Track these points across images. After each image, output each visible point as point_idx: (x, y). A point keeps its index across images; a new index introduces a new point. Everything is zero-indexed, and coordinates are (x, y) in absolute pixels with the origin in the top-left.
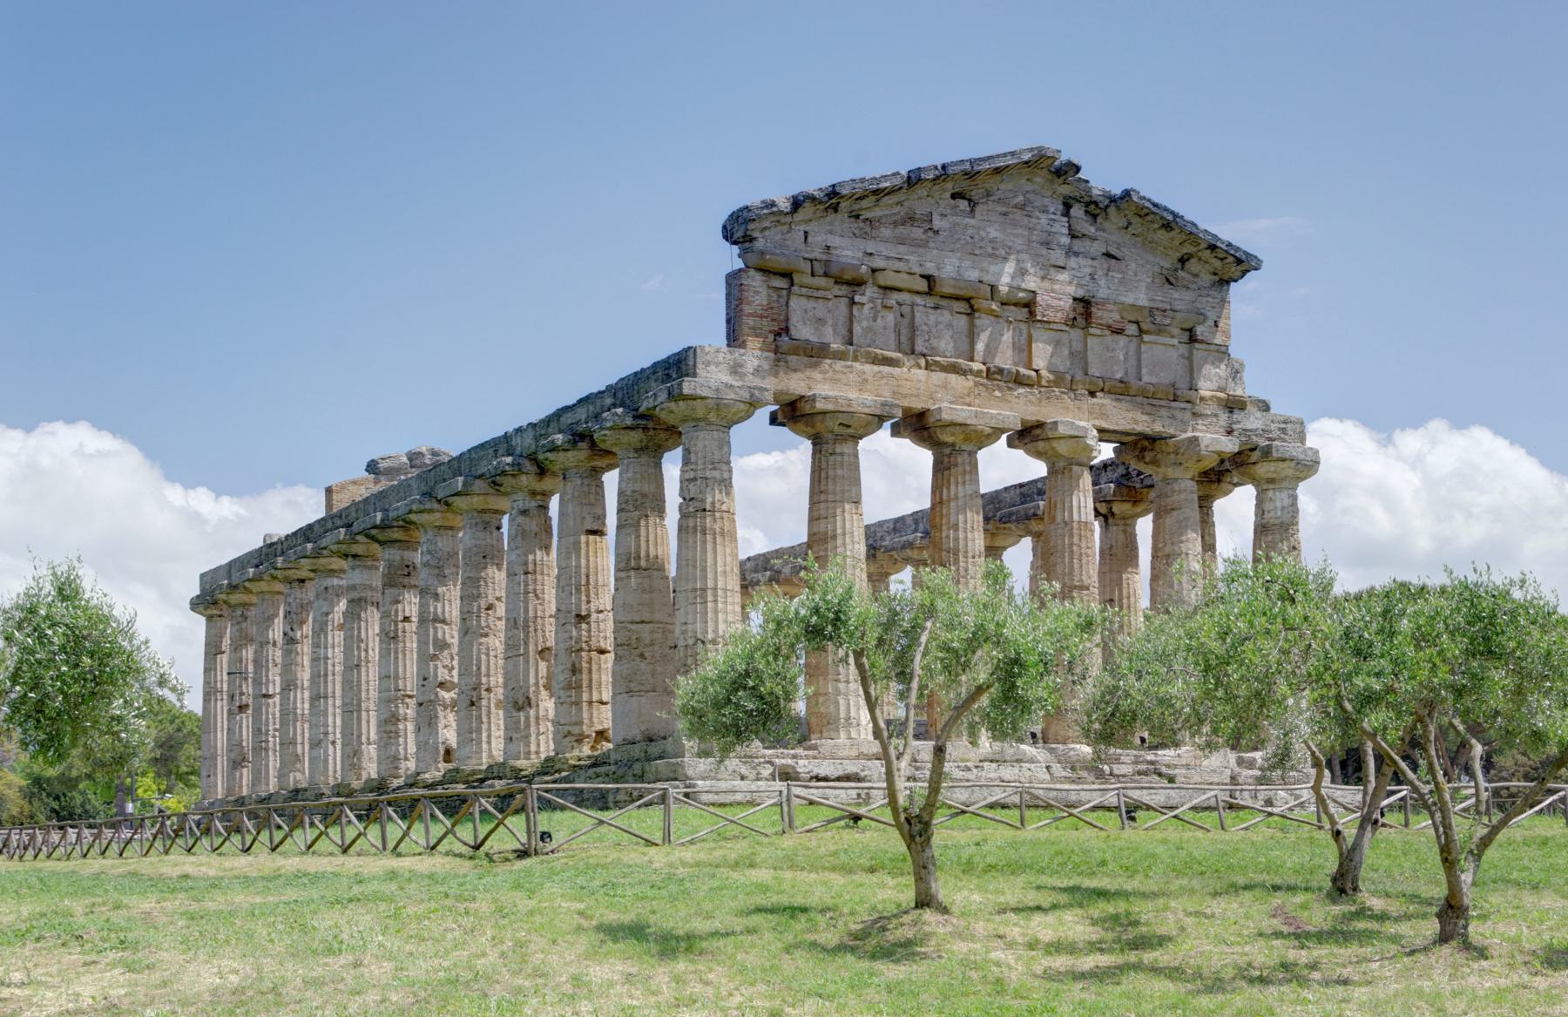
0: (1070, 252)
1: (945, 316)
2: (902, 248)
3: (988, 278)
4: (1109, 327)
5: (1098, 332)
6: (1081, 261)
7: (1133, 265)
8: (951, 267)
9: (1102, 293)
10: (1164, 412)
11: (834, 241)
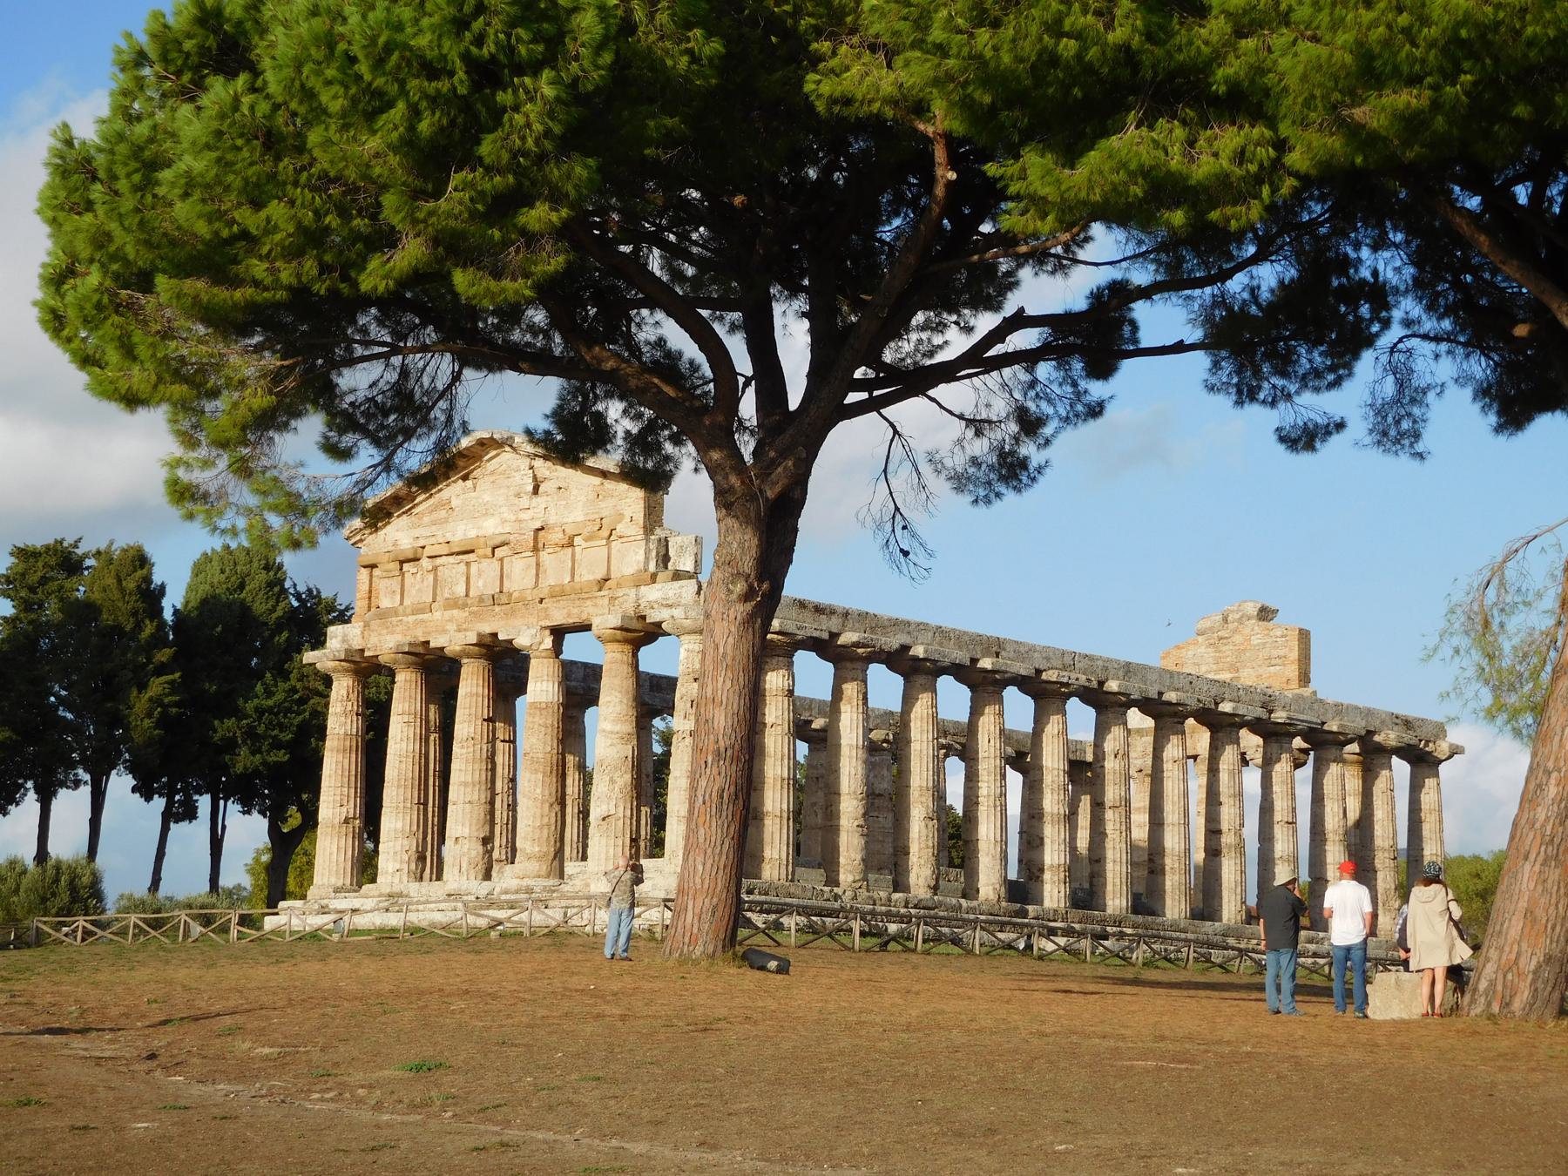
7: (575, 492)
8: (461, 532)
10: (589, 603)
11: (399, 535)
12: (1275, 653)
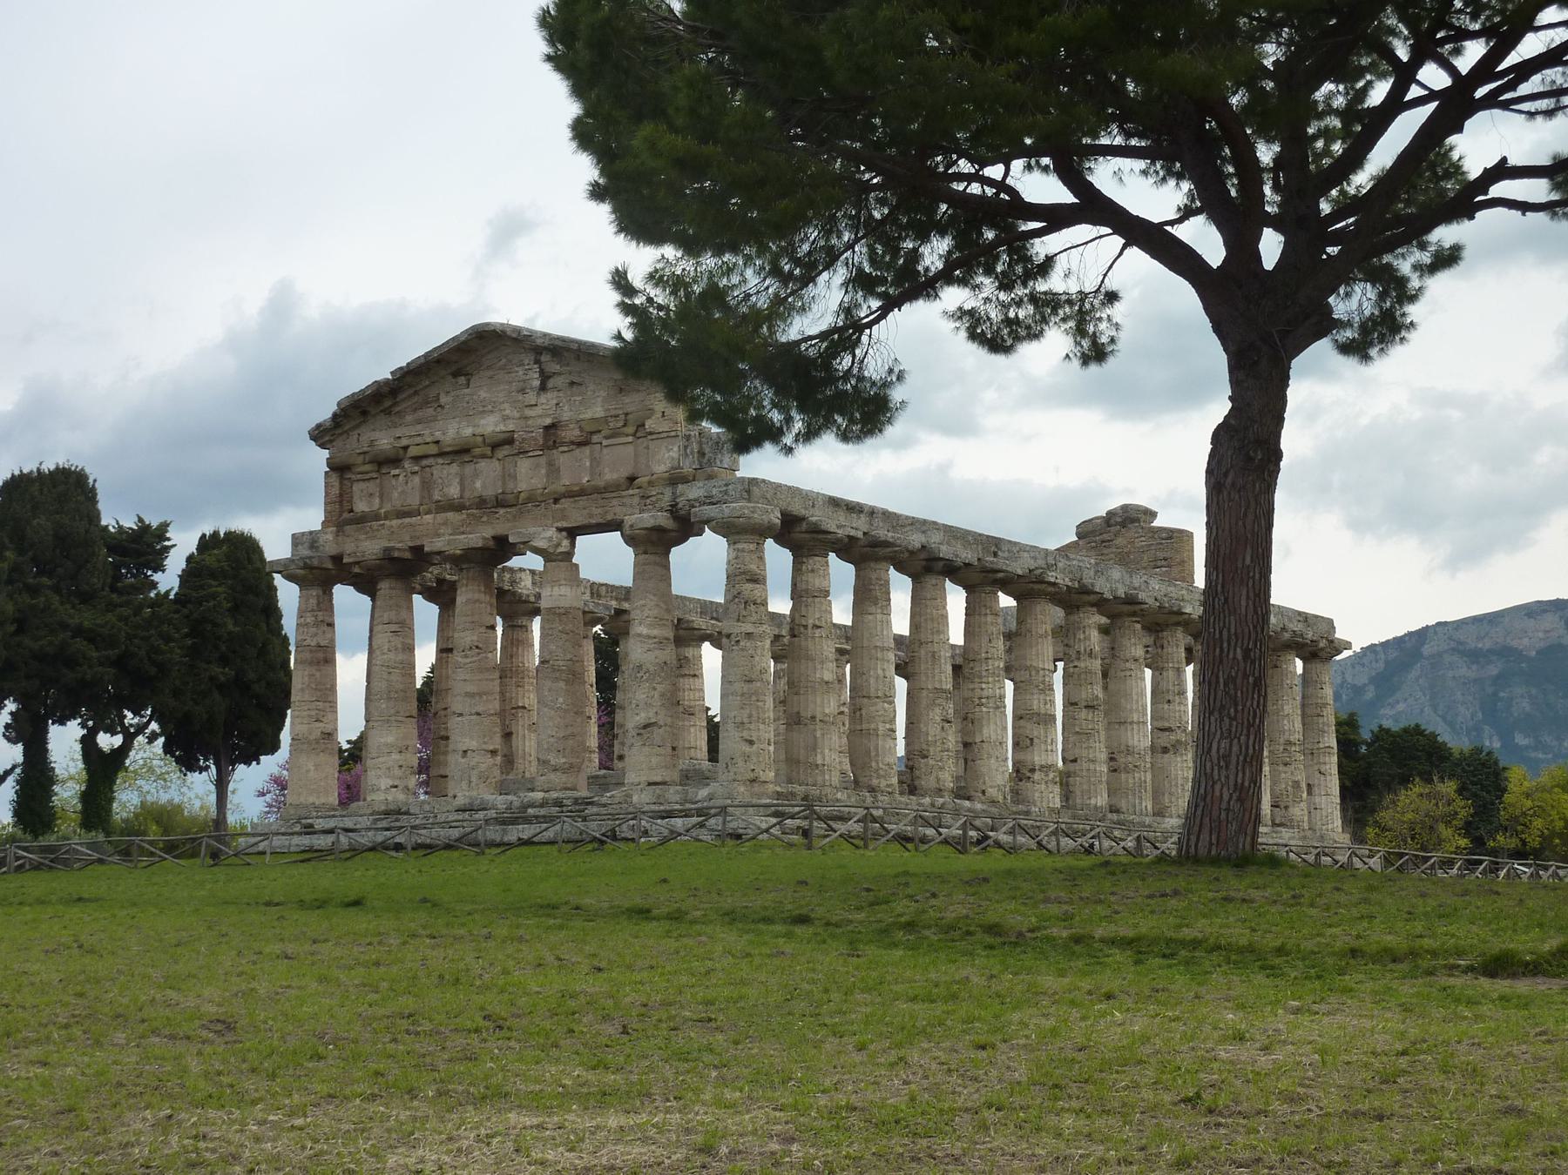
0: (543, 388)
1: (454, 468)
2: (419, 427)
3: (479, 431)
4: (572, 443)
6: (549, 395)
7: (592, 387)
8: (453, 430)
9: (566, 415)
10: (615, 502)
12: (1160, 555)
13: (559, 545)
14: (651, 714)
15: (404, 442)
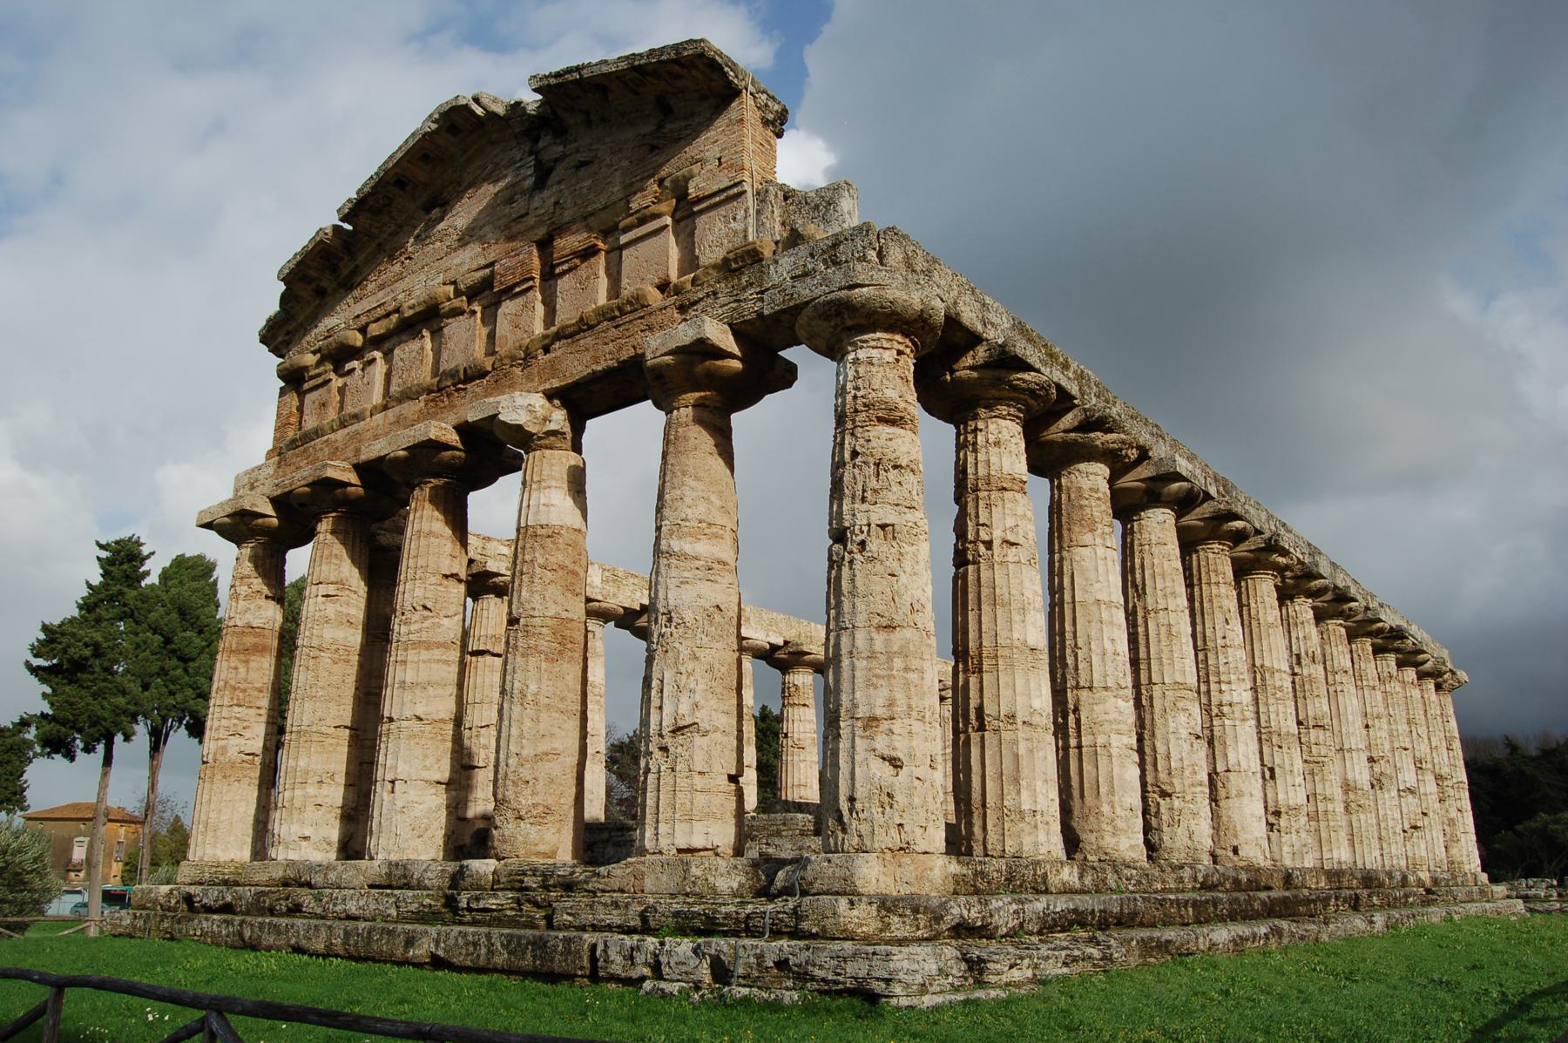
2: (381, 294)
5: (565, 267)
6: (546, 194)
13: (546, 420)
14: (684, 708)
15: (364, 320)
